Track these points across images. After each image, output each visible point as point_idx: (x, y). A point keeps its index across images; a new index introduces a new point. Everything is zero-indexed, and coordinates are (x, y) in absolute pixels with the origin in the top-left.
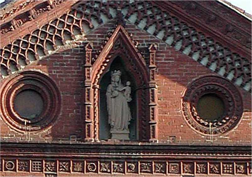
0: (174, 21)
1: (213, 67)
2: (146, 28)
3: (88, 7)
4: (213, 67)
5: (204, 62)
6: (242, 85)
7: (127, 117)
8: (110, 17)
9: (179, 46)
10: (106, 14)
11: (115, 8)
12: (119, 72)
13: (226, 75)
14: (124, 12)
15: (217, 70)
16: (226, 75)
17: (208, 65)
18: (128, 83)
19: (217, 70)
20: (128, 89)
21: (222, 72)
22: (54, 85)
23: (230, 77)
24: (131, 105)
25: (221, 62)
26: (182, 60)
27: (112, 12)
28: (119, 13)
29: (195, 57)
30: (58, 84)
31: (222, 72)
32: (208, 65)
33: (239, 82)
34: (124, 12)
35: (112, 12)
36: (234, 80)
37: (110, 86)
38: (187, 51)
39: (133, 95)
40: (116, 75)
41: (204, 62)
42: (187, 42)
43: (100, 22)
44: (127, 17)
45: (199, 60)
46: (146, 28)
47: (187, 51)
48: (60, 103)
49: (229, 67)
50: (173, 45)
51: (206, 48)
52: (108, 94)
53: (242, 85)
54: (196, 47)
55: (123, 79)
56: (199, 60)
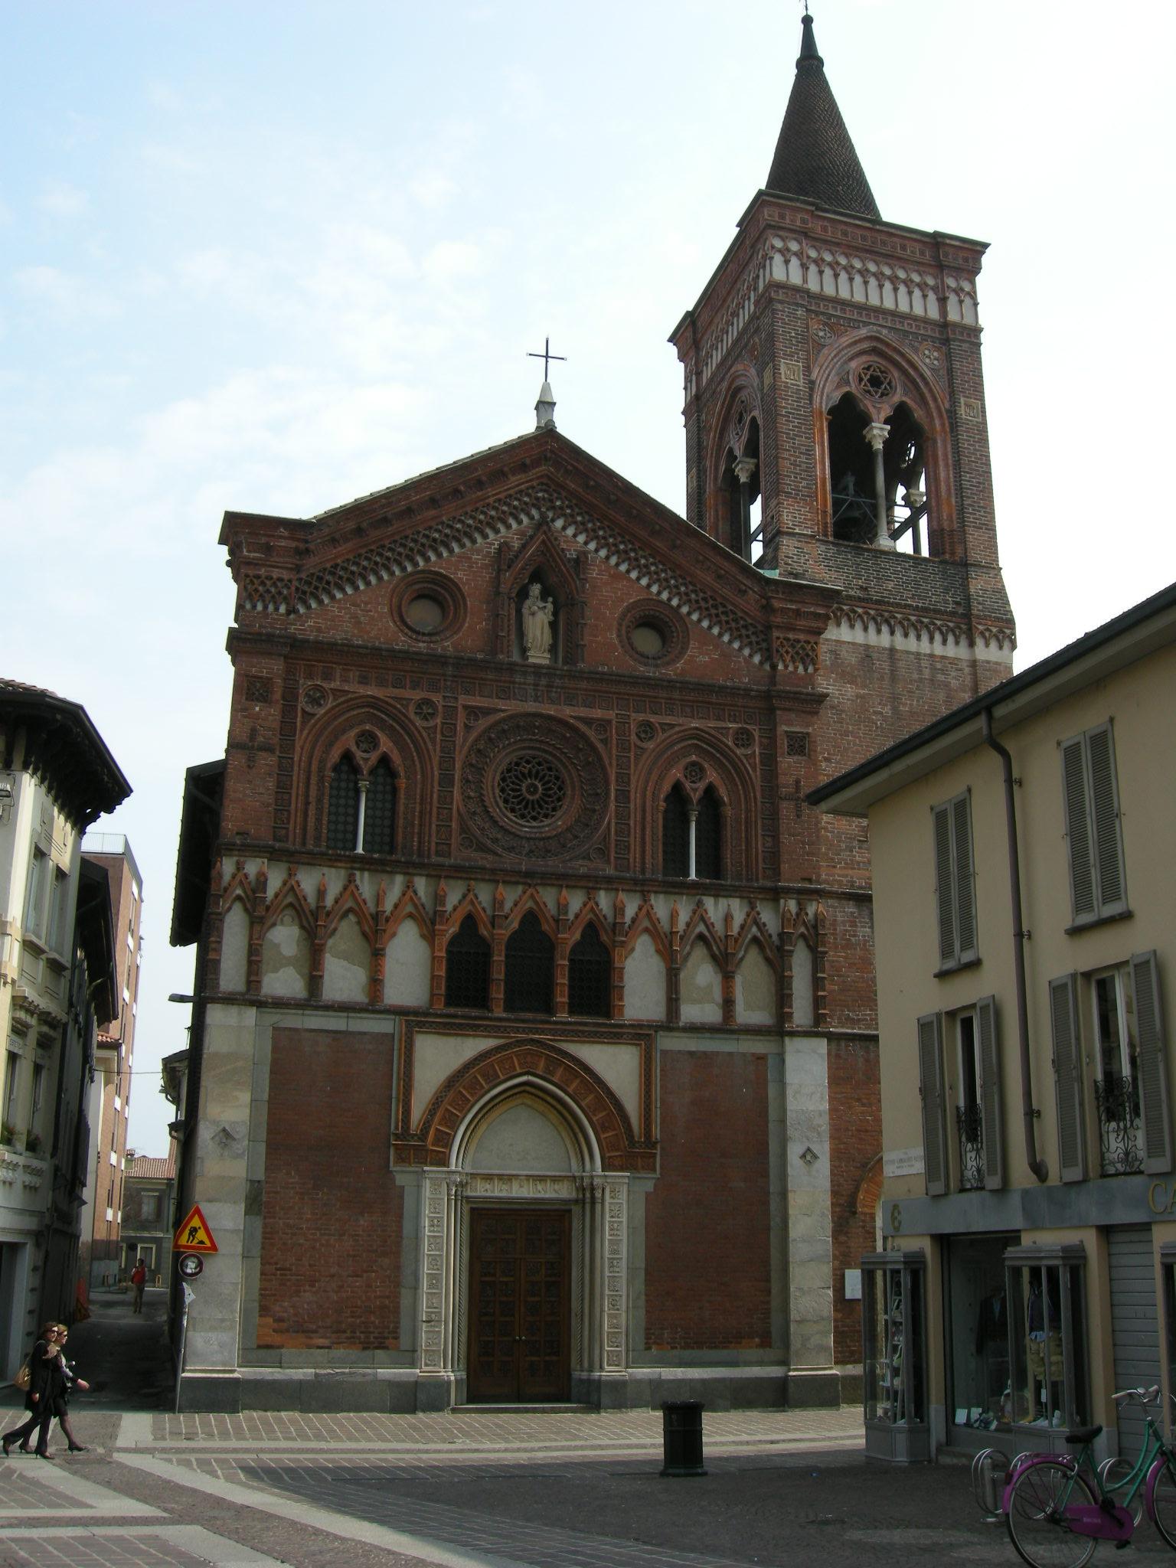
0: (609, 532)
1: (655, 589)
2: (575, 536)
3: (505, 504)
4: (655, 589)
5: (644, 582)
6: (689, 614)
7: (547, 638)
8: (532, 518)
9: (613, 560)
10: (528, 514)
11: (539, 509)
12: (539, 586)
13: (669, 599)
14: (550, 514)
15: (659, 593)
16: (669, 599)
17: (649, 586)
18: (550, 599)
19: (659, 593)
20: (550, 606)
21: (665, 596)
22: (459, 589)
23: (675, 602)
24: (553, 625)
25: (665, 585)
26: (617, 577)
27: (534, 512)
28: (543, 516)
29: (634, 575)
30: (465, 589)
31: (665, 596)
32: (649, 586)
33: (685, 610)
34: (550, 514)
35: (534, 512)
36: (679, 606)
37: (528, 602)
38: (623, 568)
39: (555, 614)
40: (536, 589)
41: (644, 582)
42: (624, 556)
43: (520, 522)
44: (553, 520)
45: (638, 579)
46: (575, 536)
47: (623, 568)
48: (465, 613)
49: (675, 591)
50: (607, 558)
51: (646, 566)
52: (525, 611)
53: (689, 614)
54: (635, 564)
55: (544, 596)
56: (638, 579)
